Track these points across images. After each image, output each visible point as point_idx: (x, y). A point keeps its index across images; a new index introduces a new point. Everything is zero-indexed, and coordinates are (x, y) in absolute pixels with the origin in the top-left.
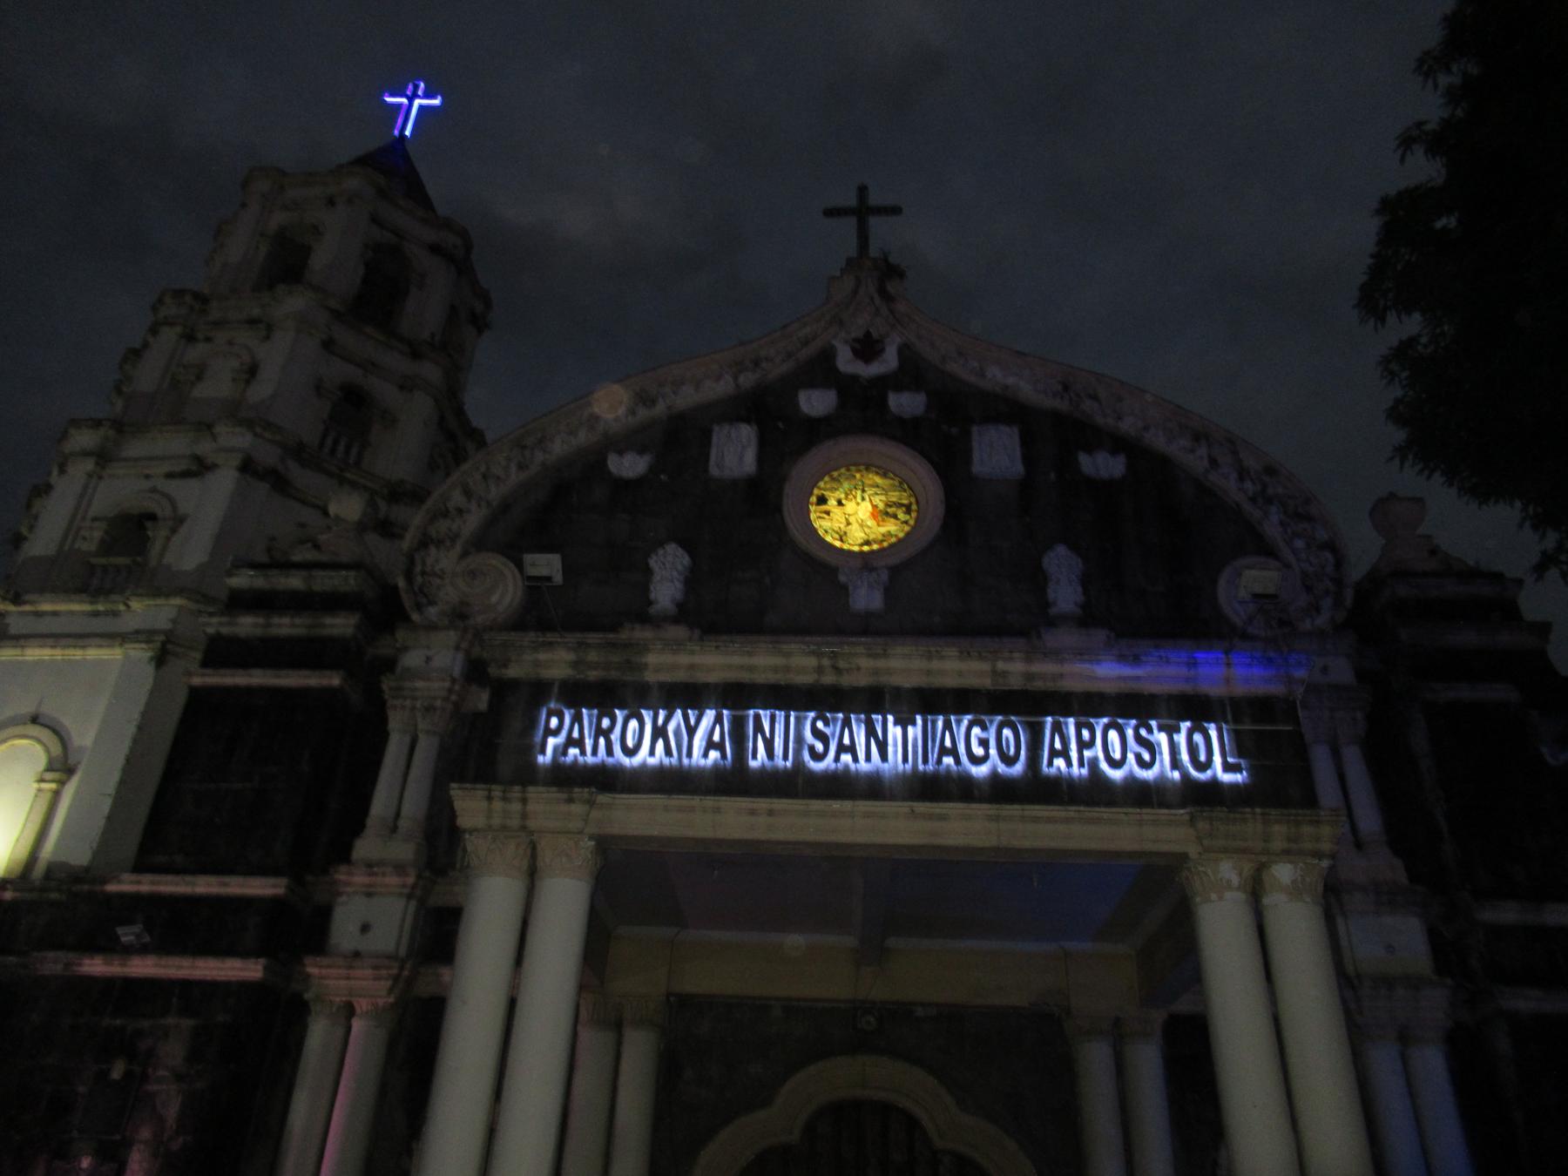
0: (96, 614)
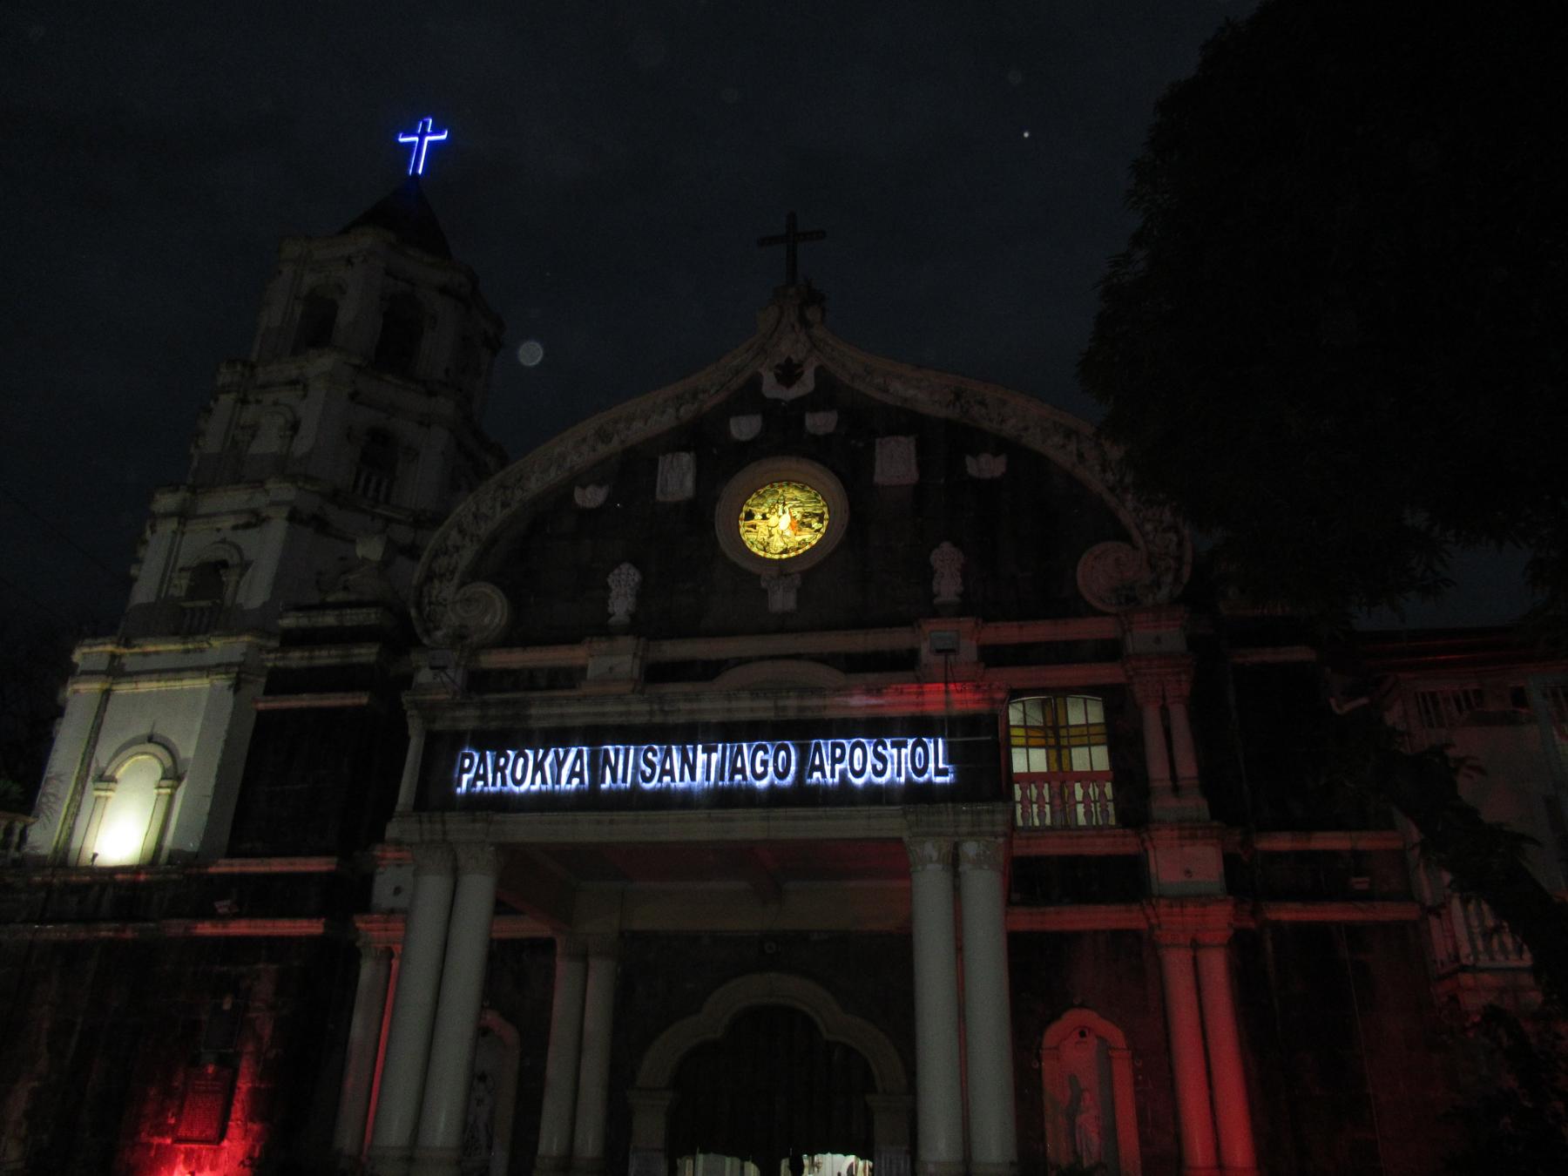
0: (187, 651)
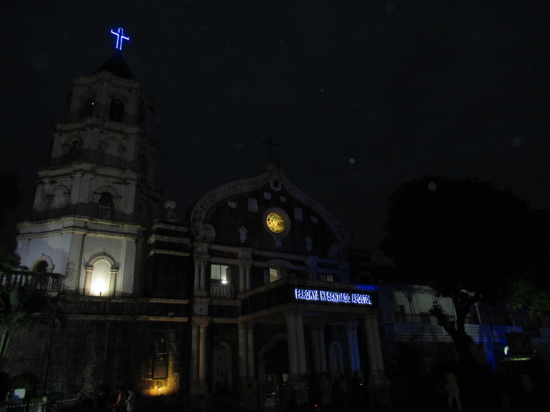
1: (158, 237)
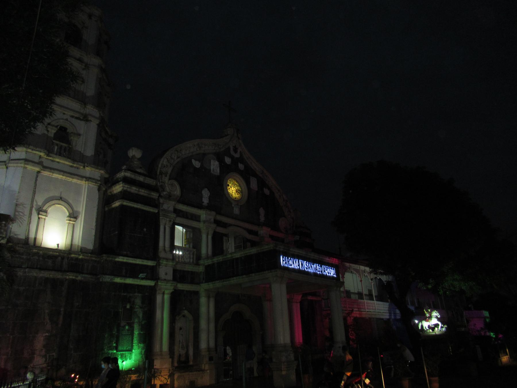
0: (72, 166)
1: (126, 186)
